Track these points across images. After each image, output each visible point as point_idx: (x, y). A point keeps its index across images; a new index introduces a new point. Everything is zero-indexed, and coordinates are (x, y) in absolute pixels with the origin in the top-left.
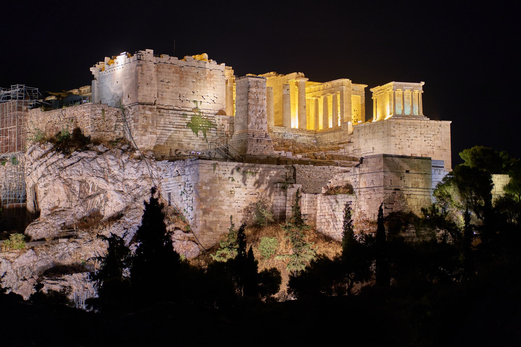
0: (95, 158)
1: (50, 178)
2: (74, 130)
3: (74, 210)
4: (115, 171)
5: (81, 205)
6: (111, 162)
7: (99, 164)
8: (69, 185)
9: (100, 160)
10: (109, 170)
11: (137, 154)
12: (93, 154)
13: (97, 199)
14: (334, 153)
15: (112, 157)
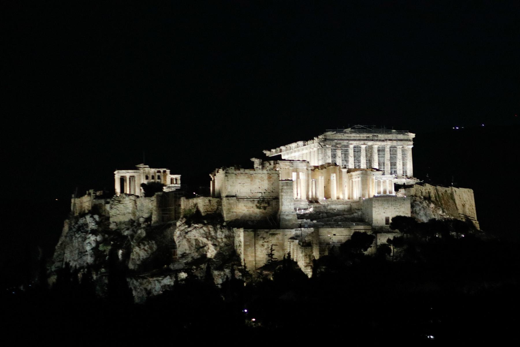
0: (202, 227)
1: (181, 238)
2: (196, 211)
3: (193, 255)
4: (213, 233)
5: (197, 252)
6: (211, 229)
7: (204, 230)
8: (189, 242)
9: (205, 228)
10: (210, 233)
11: (225, 224)
12: (200, 225)
13: (205, 248)
14: (349, 216)
15: (211, 226)
